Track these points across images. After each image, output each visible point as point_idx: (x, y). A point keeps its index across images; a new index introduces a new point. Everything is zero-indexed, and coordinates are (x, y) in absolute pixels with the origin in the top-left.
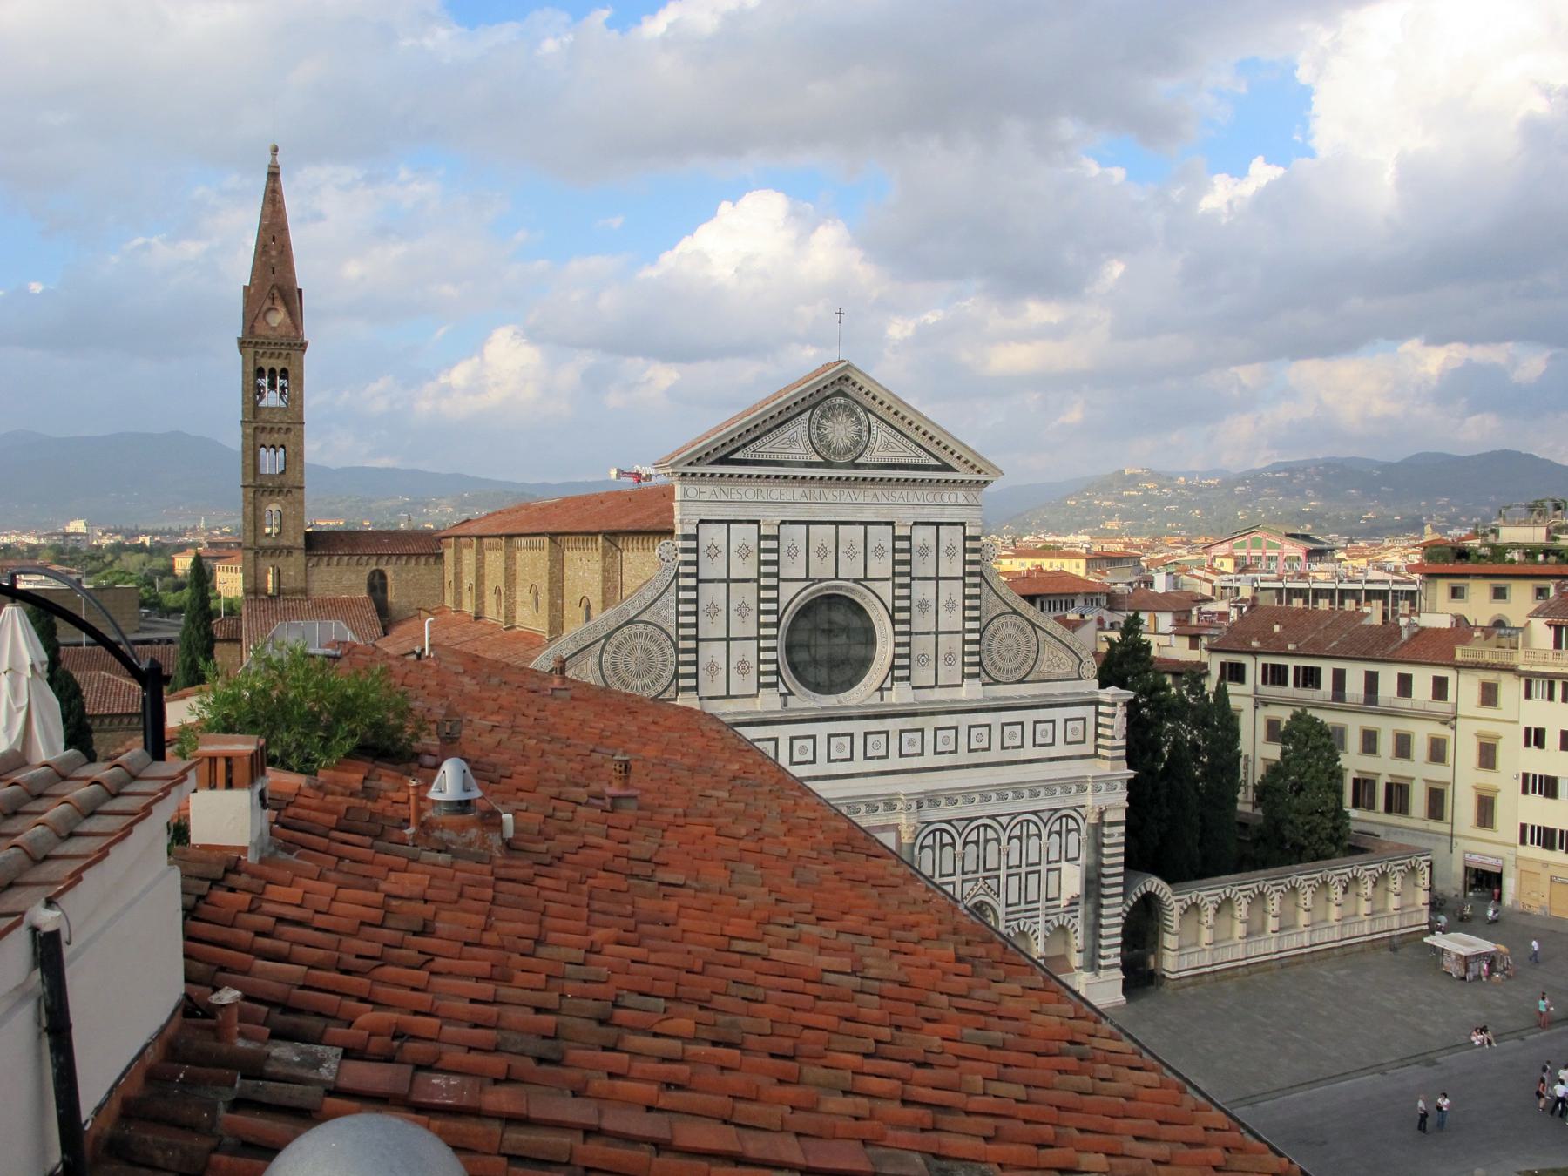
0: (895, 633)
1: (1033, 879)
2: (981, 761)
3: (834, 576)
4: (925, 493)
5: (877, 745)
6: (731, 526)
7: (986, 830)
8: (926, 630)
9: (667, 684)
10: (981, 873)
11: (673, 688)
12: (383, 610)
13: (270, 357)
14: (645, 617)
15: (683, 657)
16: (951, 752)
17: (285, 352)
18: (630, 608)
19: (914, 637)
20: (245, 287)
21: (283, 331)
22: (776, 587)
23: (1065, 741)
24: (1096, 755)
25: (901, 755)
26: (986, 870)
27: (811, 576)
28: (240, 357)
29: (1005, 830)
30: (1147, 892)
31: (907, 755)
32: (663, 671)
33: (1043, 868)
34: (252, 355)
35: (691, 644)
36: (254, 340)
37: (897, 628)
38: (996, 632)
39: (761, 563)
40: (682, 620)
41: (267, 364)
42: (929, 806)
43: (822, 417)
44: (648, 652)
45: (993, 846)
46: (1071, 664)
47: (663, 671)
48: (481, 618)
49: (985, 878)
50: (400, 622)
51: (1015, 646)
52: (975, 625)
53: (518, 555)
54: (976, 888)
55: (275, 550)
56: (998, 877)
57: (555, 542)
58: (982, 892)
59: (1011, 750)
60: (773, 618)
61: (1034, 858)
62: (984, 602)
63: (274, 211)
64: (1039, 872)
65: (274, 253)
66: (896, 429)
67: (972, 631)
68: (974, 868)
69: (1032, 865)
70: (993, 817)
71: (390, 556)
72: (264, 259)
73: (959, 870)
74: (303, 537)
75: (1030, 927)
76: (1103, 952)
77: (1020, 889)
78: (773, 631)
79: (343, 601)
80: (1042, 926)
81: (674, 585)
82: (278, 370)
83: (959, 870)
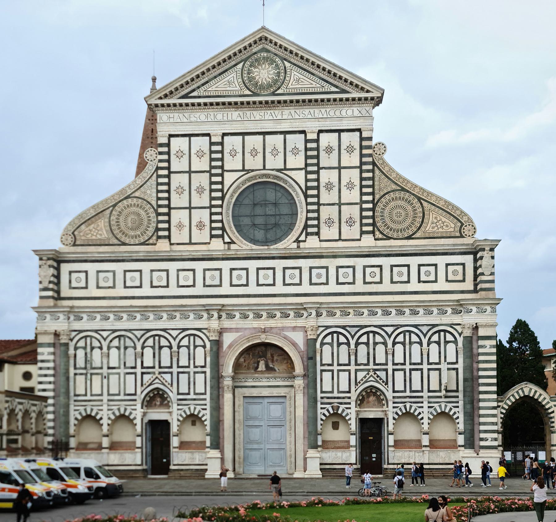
0: (307, 204)
1: (416, 375)
2: (375, 291)
3: (262, 168)
4: (328, 110)
5: (293, 276)
6: (192, 138)
7: (374, 336)
8: (331, 202)
9: (151, 235)
10: (371, 366)
11: (155, 238)
14: (137, 194)
15: (161, 218)
16: (349, 283)
18: (127, 189)
19: (321, 207)
22: (222, 175)
23: (447, 280)
24: (475, 291)
25: (311, 284)
26: (375, 364)
27: (246, 168)
29: (390, 336)
30: (525, 396)
31: (316, 284)
32: (149, 227)
33: (425, 367)
35: (165, 210)
37: (310, 200)
38: (387, 203)
39: (212, 160)
40: (160, 195)
42: (327, 315)
43: (251, 66)
44: (139, 215)
45: (380, 349)
46: (453, 226)
47: (149, 227)
49: (375, 370)
51: (403, 214)
52: (370, 198)
54: (368, 376)
56: (386, 370)
58: (372, 379)
59: (399, 284)
60: (219, 194)
61: (416, 358)
62: (376, 183)
64: (421, 370)
66: (305, 70)
67: (367, 202)
68: (366, 362)
69: (414, 364)
70: (380, 327)
73: (353, 362)
75: (416, 410)
76: (482, 435)
77: (405, 380)
78: (219, 202)
80: (425, 409)
81: (155, 175)
83: (353, 362)
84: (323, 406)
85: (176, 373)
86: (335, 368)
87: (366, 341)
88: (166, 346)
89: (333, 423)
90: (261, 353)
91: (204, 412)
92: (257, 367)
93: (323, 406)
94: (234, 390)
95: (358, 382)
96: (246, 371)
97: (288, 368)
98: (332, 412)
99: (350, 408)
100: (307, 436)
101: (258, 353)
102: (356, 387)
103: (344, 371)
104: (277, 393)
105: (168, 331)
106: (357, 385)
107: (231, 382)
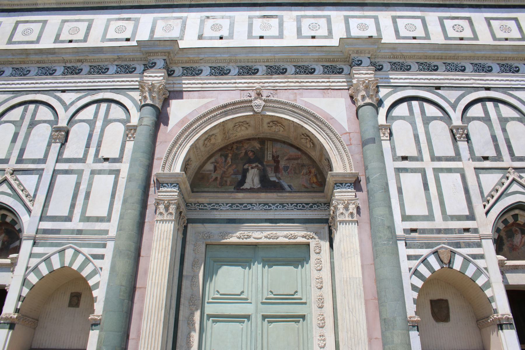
7: (496, 107)
10: (507, 162)
54: (507, 183)
58: (515, 187)
70: (504, 90)
84: (412, 252)
85: (51, 173)
86: (429, 165)
87: (482, 114)
88: (45, 122)
89: (431, 301)
90: (251, 154)
91: (98, 263)
92: (243, 181)
93: (412, 252)
94: (186, 227)
95: (486, 194)
96: (216, 190)
97: (311, 184)
98: (437, 266)
99: (482, 257)
100: (378, 334)
101: (246, 153)
102: (485, 206)
103: (449, 170)
104: (286, 237)
105: (59, 94)
106: (488, 202)
107: (177, 194)
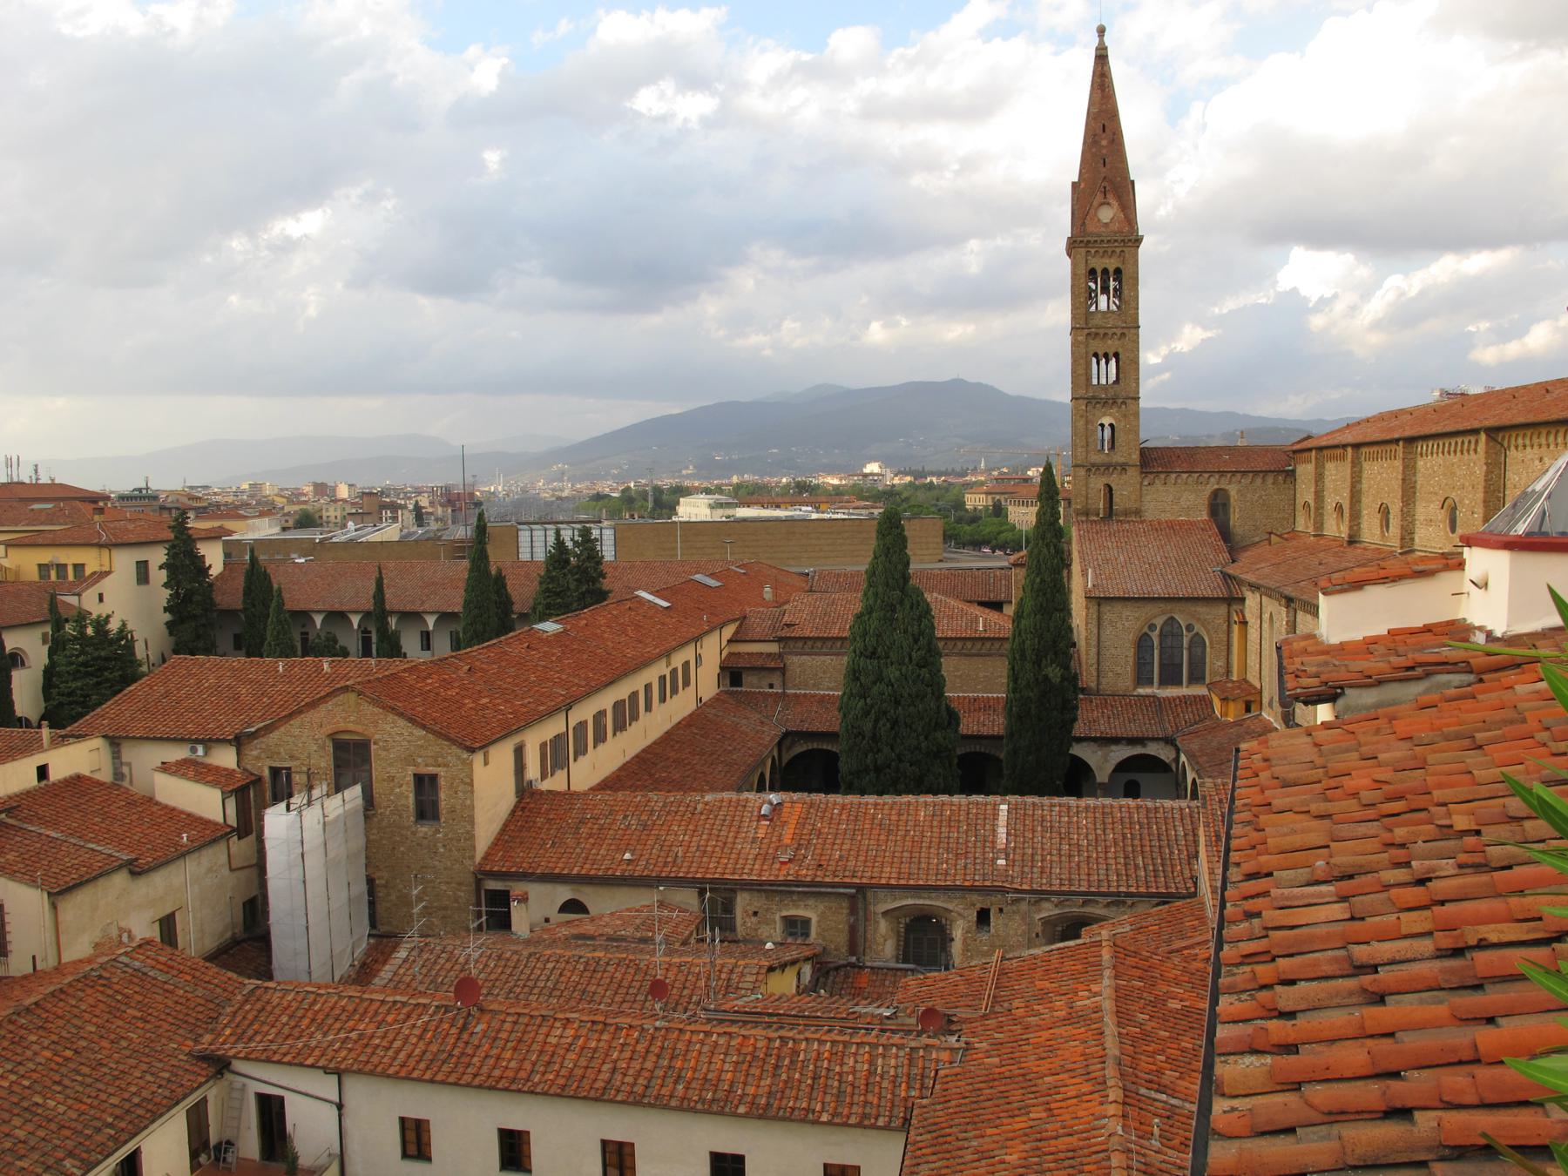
12: (1226, 534)
13: (1102, 257)
17: (1118, 250)
20: (1073, 183)
21: (1116, 227)
28: (1068, 261)
34: (1084, 254)
36: (1085, 239)
41: (1099, 264)
48: (1356, 542)
50: (1245, 548)
53: (1420, 463)
55: (1108, 468)
57: (1496, 441)
63: (1103, 97)
65: (1104, 143)
71: (1234, 473)
72: (1094, 150)
74: (1138, 452)
79: (1181, 524)
82: (1111, 270)
